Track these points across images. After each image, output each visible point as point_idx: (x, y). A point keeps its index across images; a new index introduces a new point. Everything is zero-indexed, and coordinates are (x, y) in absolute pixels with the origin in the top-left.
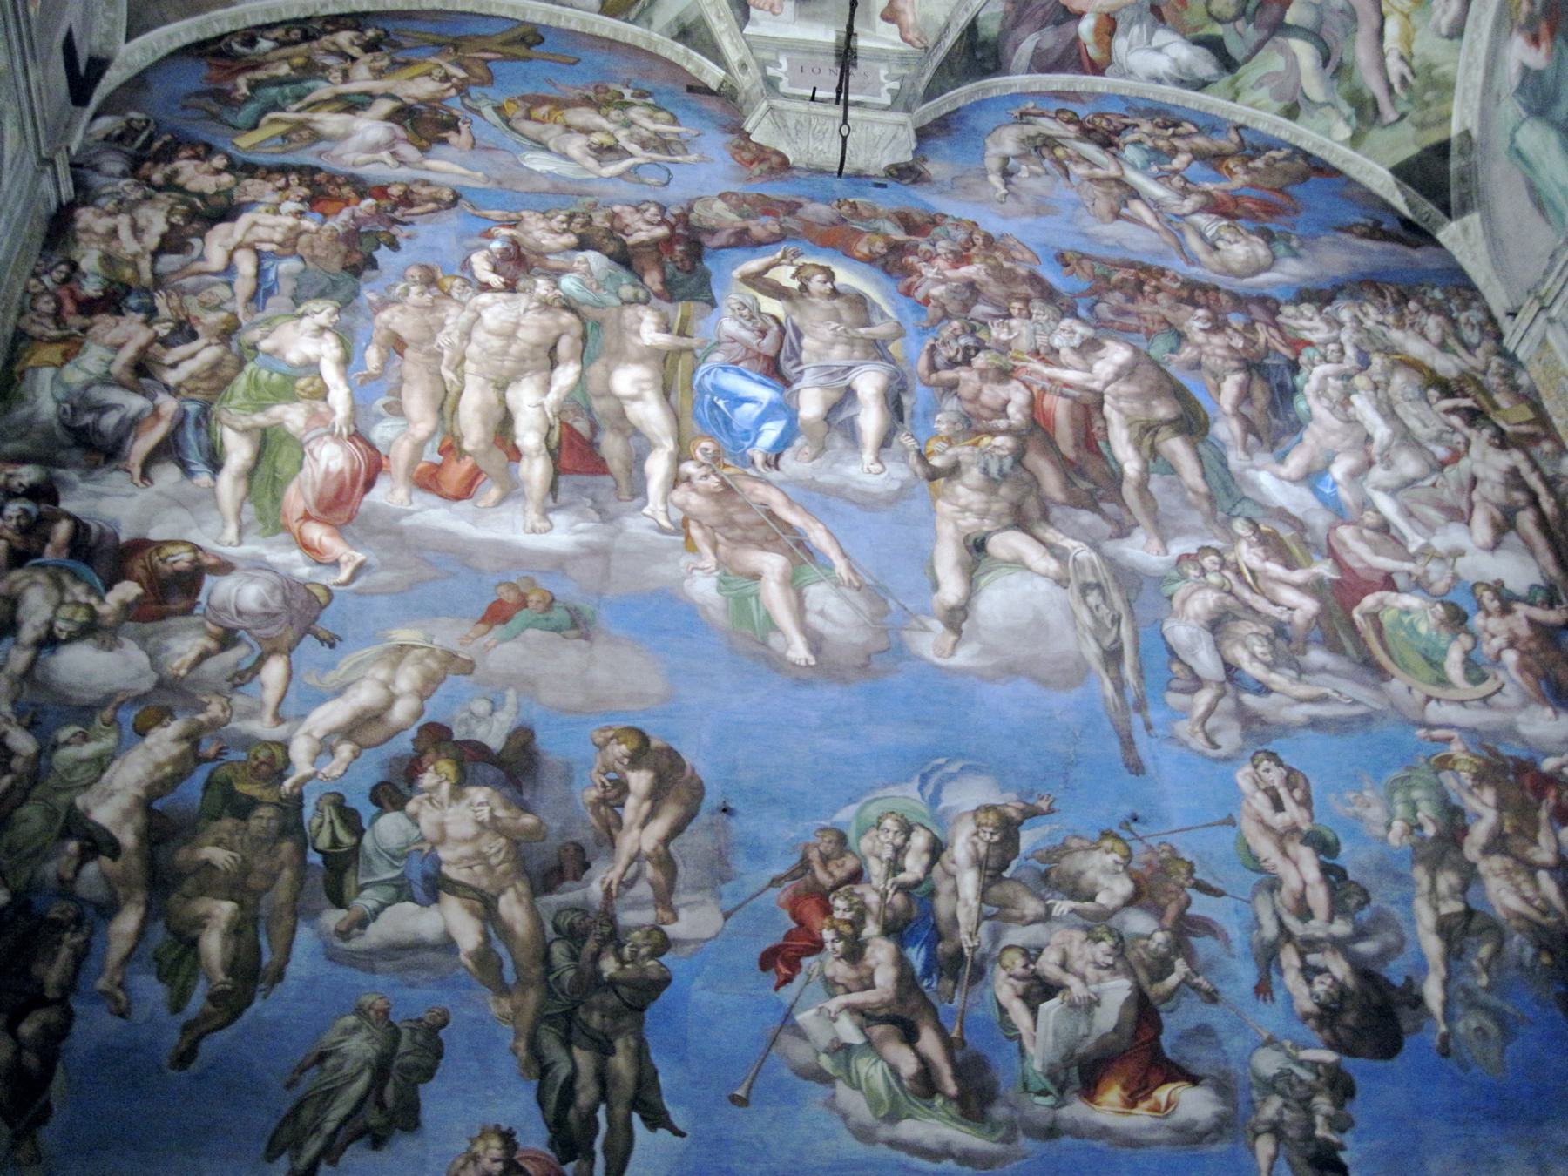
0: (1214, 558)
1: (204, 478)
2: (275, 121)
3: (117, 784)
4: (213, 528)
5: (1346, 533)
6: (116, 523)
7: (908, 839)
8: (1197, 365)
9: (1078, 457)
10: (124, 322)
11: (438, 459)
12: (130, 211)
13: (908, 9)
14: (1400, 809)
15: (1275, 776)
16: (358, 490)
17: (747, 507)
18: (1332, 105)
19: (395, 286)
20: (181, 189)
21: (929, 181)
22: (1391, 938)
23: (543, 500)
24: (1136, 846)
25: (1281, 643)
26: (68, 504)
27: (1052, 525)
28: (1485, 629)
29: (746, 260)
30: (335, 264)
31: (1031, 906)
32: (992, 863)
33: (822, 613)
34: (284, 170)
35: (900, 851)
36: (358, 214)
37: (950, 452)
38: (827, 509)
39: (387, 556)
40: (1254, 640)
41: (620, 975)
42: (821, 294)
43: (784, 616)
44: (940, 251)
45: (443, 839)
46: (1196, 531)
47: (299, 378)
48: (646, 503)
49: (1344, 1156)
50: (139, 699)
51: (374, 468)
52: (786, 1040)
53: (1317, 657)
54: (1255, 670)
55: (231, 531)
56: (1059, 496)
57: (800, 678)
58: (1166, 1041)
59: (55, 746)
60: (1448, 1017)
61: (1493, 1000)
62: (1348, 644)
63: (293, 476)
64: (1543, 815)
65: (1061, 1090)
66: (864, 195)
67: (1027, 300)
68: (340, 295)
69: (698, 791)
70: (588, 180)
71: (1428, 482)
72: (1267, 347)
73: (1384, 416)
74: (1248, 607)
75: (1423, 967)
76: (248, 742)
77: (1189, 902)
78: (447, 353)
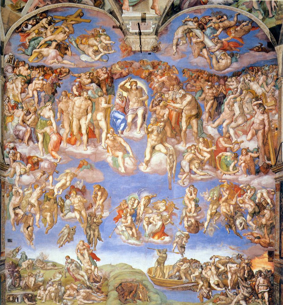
0: (194, 147)
1: (36, 144)
2: (35, 52)
3: (33, 197)
4: (39, 153)
5: (221, 139)
6: (25, 153)
7: (135, 201)
8: (204, 99)
9: (175, 126)
11: (70, 137)
14: (211, 195)
15: (192, 190)
16: (59, 144)
18: (259, 10)
20: (22, 75)
21: (160, 50)
22: (202, 216)
23: (86, 144)
25: (201, 164)
28: (241, 159)
30: (50, 93)
31: (151, 211)
32: (146, 205)
33: (127, 163)
34: (38, 67)
35: (133, 203)
36: (53, 78)
37: (152, 127)
39: (64, 157)
40: (196, 164)
41: (97, 221)
44: (159, 73)
45: (74, 203)
46: (192, 141)
48: (102, 143)
49: (185, 246)
53: (207, 167)
54: (194, 170)
55: (42, 154)
57: (123, 175)
58: (165, 230)
61: (215, 226)
62: (213, 164)
64: (236, 195)
66: (146, 58)
67: (174, 85)
68: (52, 100)
70: (93, 62)
71: (242, 125)
73: (240, 108)
74: (197, 157)
75: (206, 220)
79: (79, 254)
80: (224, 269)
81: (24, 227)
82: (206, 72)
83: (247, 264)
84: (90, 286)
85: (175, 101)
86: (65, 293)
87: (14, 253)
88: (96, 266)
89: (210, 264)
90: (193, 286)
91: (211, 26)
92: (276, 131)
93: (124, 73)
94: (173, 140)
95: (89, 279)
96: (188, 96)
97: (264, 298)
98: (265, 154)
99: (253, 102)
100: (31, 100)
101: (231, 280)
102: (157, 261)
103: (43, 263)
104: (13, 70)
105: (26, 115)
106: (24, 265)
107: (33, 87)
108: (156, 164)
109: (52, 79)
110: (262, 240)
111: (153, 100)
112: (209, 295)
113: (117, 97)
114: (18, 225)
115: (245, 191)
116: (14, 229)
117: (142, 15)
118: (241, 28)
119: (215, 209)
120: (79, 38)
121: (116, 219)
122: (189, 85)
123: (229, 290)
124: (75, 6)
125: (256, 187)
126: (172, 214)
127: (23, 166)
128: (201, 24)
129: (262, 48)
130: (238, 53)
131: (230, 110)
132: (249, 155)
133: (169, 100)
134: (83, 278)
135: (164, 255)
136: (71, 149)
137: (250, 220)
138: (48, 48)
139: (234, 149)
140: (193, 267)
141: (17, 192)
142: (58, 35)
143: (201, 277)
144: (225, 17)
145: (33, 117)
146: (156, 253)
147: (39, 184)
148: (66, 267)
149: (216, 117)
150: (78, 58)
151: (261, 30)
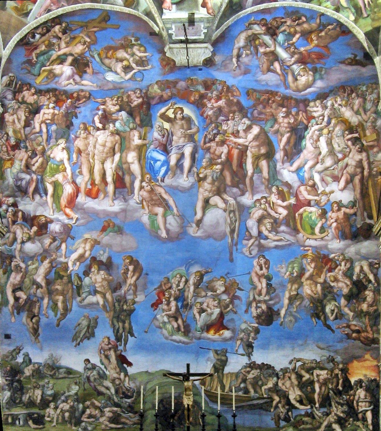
0: (265, 200)
2: (44, 71)
3: (40, 273)
4: (48, 211)
5: (302, 188)
8: (277, 132)
10: (21, 151)
11: (90, 187)
12: (16, 113)
13: (209, 2)
14: (290, 269)
15: (262, 261)
17: (156, 195)
19: (77, 131)
21: (215, 65)
22: (277, 300)
24: (228, 280)
25: (274, 225)
26: (20, 208)
27: (226, 193)
28: (330, 217)
29: (161, 108)
30: (64, 126)
31: (203, 294)
32: (197, 284)
33: (170, 224)
34: (48, 91)
35: (179, 282)
36: (68, 106)
38: (174, 193)
40: (268, 224)
42: (180, 119)
43: (162, 226)
44: (214, 95)
46: (261, 192)
47: (60, 166)
49: (253, 345)
50: (41, 254)
51: (77, 190)
52: (155, 321)
53: (283, 228)
54: (266, 233)
56: (229, 184)
58: (225, 321)
59: (28, 266)
60: (284, 317)
61: (296, 314)
62: (291, 224)
63: (61, 196)
64: (325, 270)
65: (202, 331)
66: (195, 74)
67: (234, 112)
68: (66, 136)
69: (142, 269)
70: (122, 82)
71: (332, 168)
72: (300, 121)
73: (327, 144)
74: (269, 214)
75: (282, 307)
76: (61, 263)
77: (236, 292)
78: (90, 153)
79: (103, 356)
80: (310, 378)
81: (28, 317)
82: (279, 94)
83: (342, 370)
84: (119, 402)
85: (236, 135)
86: (83, 412)
87: (14, 354)
88: (126, 374)
89: (288, 370)
90: (266, 403)
91: (285, 31)
92: (379, 177)
93: (165, 96)
94: (235, 190)
95: (117, 392)
96: (254, 127)
97: (366, 421)
98: (365, 209)
99: (346, 135)
100: (38, 137)
101: (319, 394)
102: (214, 366)
103: (53, 369)
104: (14, 96)
105: (31, 158)
106: (28, 371)
107: (41, 119)
108: (211, 225)
109: (66, 107)
110: (363, 334)
111: (206, 133)
112: (288, 415)
113: (155, 129)
114: (18, 313)
115: (338, 262)
116: (13, 320)
117: (189, 16)
118: (326, 34)
119: (295, 290)
120: (104, 50)
121: (155, 305)
122: (256, 111)
123: (316, 408)
124: (98, 8)
125: (353, 258)
126: (234, 298)
127: (26, 230)
128: (271, 28)
129: (357, 61)
130: (322, 68)
131: (314, 146)
132: (342, 211)
133: (229, 134)
134: (108, 391)
135: (224, 358)
136: (91, 204)
137: (346, 306)
138: (62, 64)
139: (321, 203)
140: (265, 376)
141: (17, 266)
142: (76, 48)
143: (275, 389)
144: (304, 19)
145: (40, 160)
146: (211, 354)
147: (47, 255)
148: (85, 374)
149: (295, 158)
150: (103, 76)
151: (354, 36)
